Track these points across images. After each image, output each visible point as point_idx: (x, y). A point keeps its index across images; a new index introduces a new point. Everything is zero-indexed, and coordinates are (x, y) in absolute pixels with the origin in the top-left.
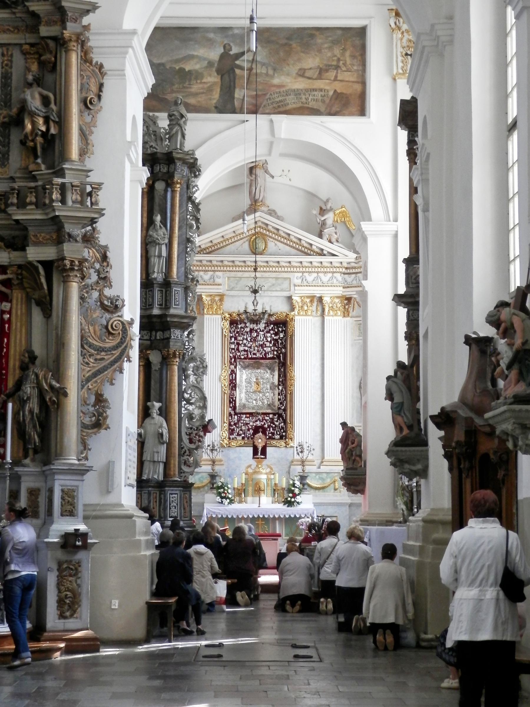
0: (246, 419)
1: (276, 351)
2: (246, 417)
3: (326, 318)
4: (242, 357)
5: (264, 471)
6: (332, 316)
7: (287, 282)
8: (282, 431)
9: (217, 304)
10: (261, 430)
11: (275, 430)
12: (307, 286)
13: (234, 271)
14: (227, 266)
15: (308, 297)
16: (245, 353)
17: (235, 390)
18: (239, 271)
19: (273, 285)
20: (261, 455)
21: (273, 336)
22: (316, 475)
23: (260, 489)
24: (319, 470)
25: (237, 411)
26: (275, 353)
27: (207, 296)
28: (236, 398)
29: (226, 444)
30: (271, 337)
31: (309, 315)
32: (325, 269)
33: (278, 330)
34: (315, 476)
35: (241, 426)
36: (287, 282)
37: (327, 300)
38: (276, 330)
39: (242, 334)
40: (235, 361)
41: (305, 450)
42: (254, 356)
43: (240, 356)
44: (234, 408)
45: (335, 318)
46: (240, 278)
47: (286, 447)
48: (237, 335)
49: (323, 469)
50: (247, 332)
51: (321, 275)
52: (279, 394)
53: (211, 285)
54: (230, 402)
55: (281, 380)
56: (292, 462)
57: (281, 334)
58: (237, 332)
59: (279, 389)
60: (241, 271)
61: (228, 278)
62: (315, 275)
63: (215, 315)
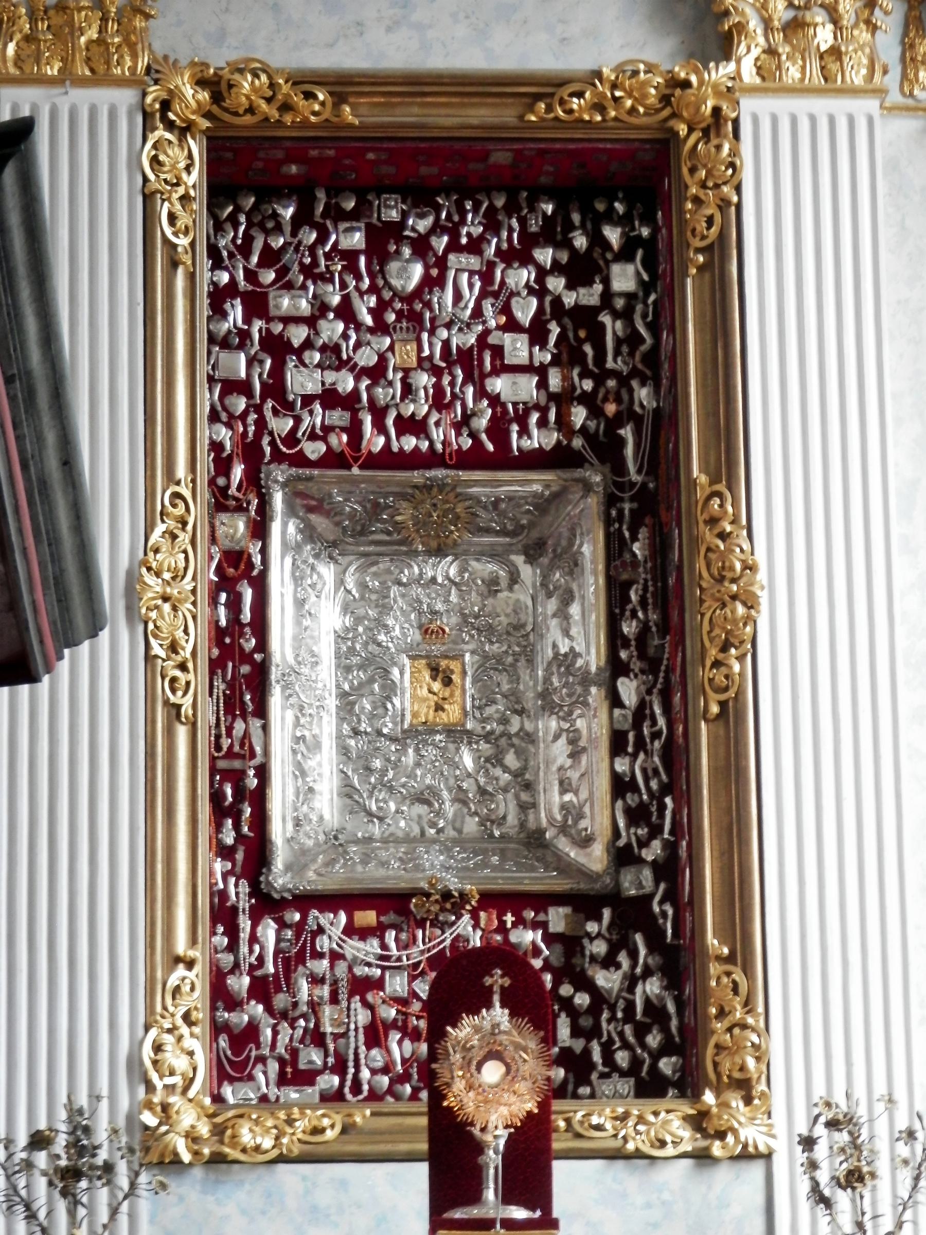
0: (354, 948)
1: (587, 400)
2: (350, 930)
4: (314, 450)
8: (653, 1040)
10: (497, 979)
11: (594, 1032)
16: (338, 417)
17: (261, 711)
20: (509, 1197)
21: (556, 284)
26: (579, 415)
28: (263, 772)
29: (192, 1137)
30: (539, 290)
33: (598, 240)
35: (314, 1006)
38: (580, 242)
39: (309, 271)
40: (253, 479)
41: (883, 1166)
42: (410, 443)
43: (291, 439)
47: (702, 1157)
48: (269, 276)
50: (350, 256)
52: (618, 744)
54: (220, 811)
55: (629, 628)
57: (616, 268)
58: (270, 257)
59: (615, 701)
63: (82, 82)
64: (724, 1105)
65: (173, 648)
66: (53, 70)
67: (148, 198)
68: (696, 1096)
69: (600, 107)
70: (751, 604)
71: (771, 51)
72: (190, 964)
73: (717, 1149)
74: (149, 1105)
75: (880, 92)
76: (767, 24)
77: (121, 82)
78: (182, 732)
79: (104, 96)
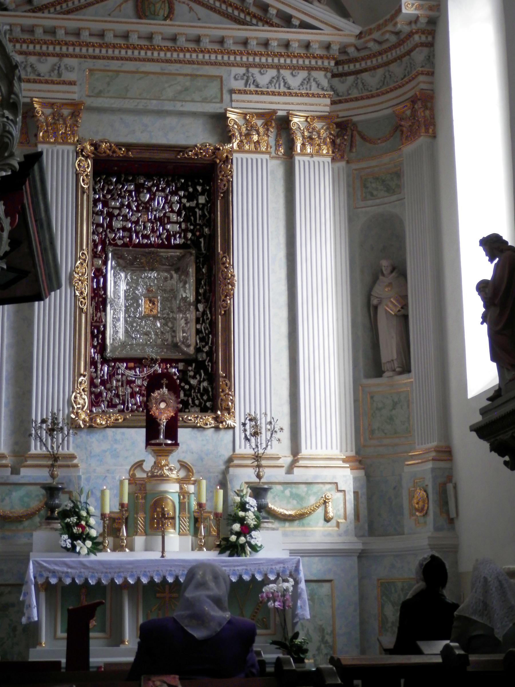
0: (128, 372)
1: (192, 231)
2: (127, 368)
3: (297, 158)
4: (120, 242)
5: (174, 475)
6: (312, 156)
7: (216, 84)
8: (205, 398)
9: (65, 123)
10: (165, 381)
11: (190, 395)
12: (257, 93)
13: (104, 58)
14: (87, 45)
15: (260, 115)
16: (126, 234)
17: (105, 310)
18: (113, 58)
19: (186, 89)
20: (166, 437)
21: (184, 201)
22: (285, 489)
23: (163, 515)
24: (290, 478)
25: (109, 353)
26: (189, 235)
27: (43, 105)
28: (105, 326)
29: (84, 421)
30: (180, 202)
31: (262, 153)
32: (295, 61)
33: (195, 190)
34: (283, 492)
35: (117, 387)
36: (216, 84)
37: (297, 121)
38: (191, 190)
39: (120, 196)
40: (103, 250)
41: (263, 431)
42: (145, 241)
43: (114, 239)
44: (102, 348)
45: (316, 159)
46: (118, 72)
47: (217, 428)
49: (298, 474)
50: (130, 192)
51: (286, 73)
52: (197, 321)
53: (53, 82)
54: (93, 336)
55: (201, 291)
56: (230, 460)
57: (200, 197)
58: (109, 191)
59: (197, 309)
60: (117, 59)
61: (91, 70)
62: (273, 73)
63: (60, 144)
64: (223, 414)
65: (81, 293)
66: (52, 140)
67: (77, 175)
68: (216, 412)
69: (196, 154)
70: (233, 285)
71: (241, 141)
72: (84, 376)
73: (221, 426)
74: (73, 413)
75: (269, 153)
76: (241, 135)
77: (70, 144)
78: (83, 316)
79: (66, 148)
